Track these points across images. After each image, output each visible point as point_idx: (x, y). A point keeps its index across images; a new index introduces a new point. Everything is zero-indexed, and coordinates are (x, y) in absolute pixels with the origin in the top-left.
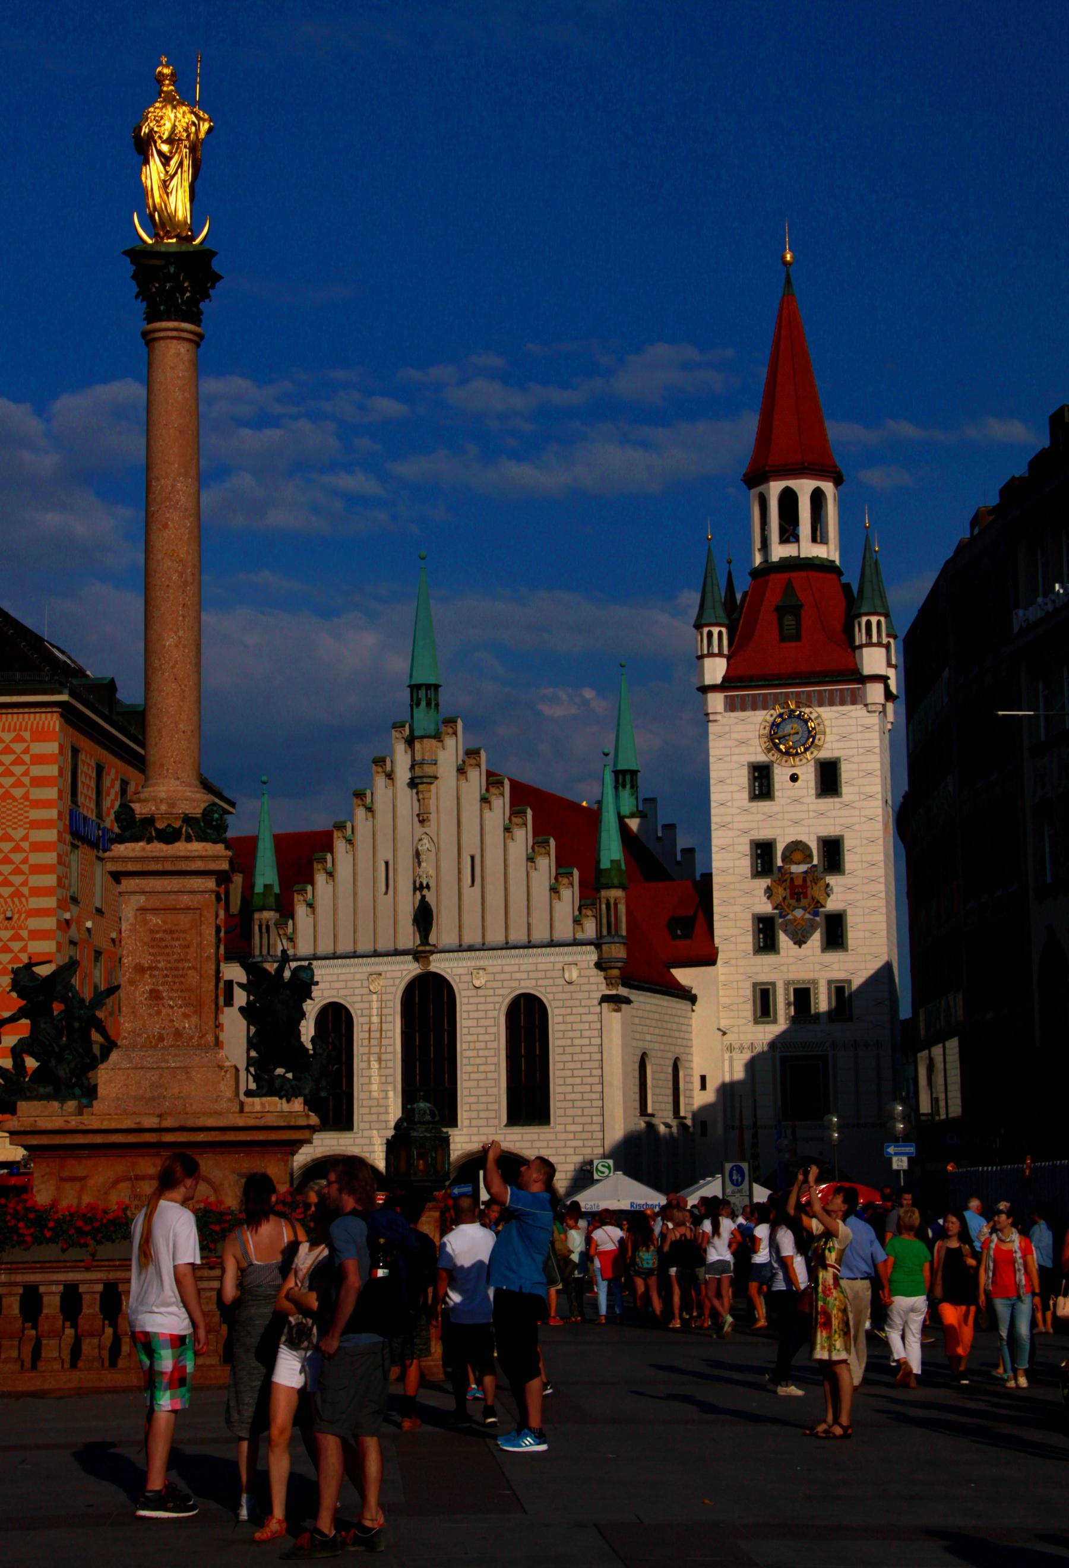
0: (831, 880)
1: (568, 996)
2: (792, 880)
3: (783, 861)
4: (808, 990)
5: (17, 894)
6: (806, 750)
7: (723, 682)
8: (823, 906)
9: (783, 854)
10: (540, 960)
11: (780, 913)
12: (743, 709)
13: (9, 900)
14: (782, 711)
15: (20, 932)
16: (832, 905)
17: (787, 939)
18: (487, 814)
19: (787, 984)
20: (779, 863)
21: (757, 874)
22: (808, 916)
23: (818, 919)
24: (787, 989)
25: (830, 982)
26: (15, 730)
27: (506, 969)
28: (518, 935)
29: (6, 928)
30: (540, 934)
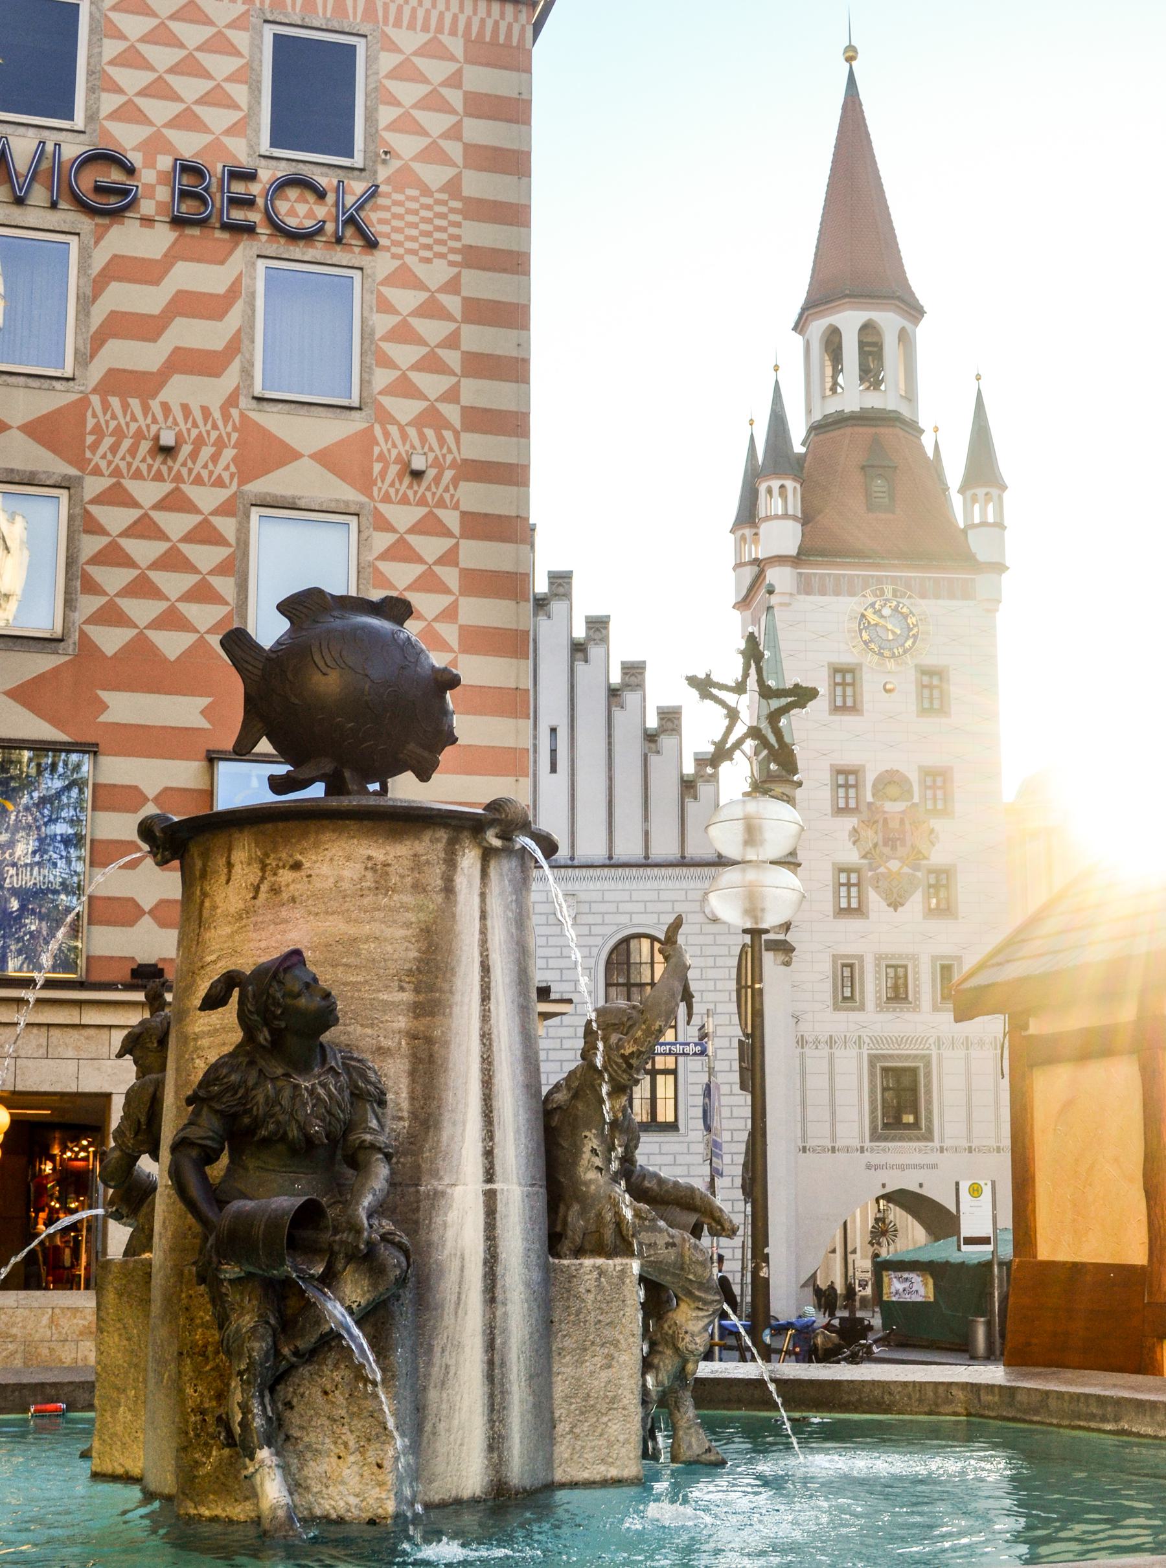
0: (936, 824)
1: (709, 939)
2: (885, 821)
3: (874, 795)
4: (905, 967)
5: (431, 418)
6: (905, 652)
7: (798, 554)
8: (925, 858)
9: (874, 786)
10: (663, 885)
11: (870, 864)
12: (823, 593)
13: (412, 432)
14: (874, 599)
15: (440, 512)
16: (938, 857)
17: (878, 898)
18: (580, 666)
19: (878, 958)
20: (869, 798)
21: (839, 811)
22: (906, 870)
23: (919, 874)
24: (878, 965)
25: (934, 959)
26: (426, 28)
27: (608, 896)
28: (628, 847)
29: (405, 501)
30: (665, 846)
